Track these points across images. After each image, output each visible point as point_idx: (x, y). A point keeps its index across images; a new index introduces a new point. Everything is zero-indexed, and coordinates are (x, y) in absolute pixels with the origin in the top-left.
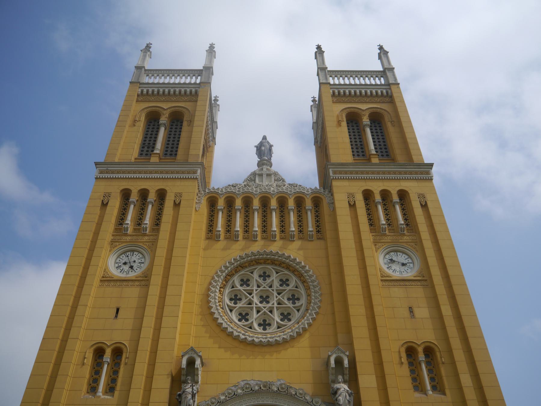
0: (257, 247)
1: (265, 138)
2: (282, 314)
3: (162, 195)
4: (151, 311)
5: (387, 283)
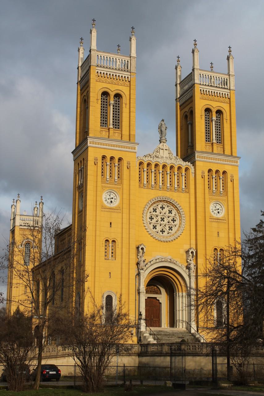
0: (161, 194)
1: (163, 120)
2: (169, 227)
3: (120, 159)
4: (126, 226)
5: (213, 220)
